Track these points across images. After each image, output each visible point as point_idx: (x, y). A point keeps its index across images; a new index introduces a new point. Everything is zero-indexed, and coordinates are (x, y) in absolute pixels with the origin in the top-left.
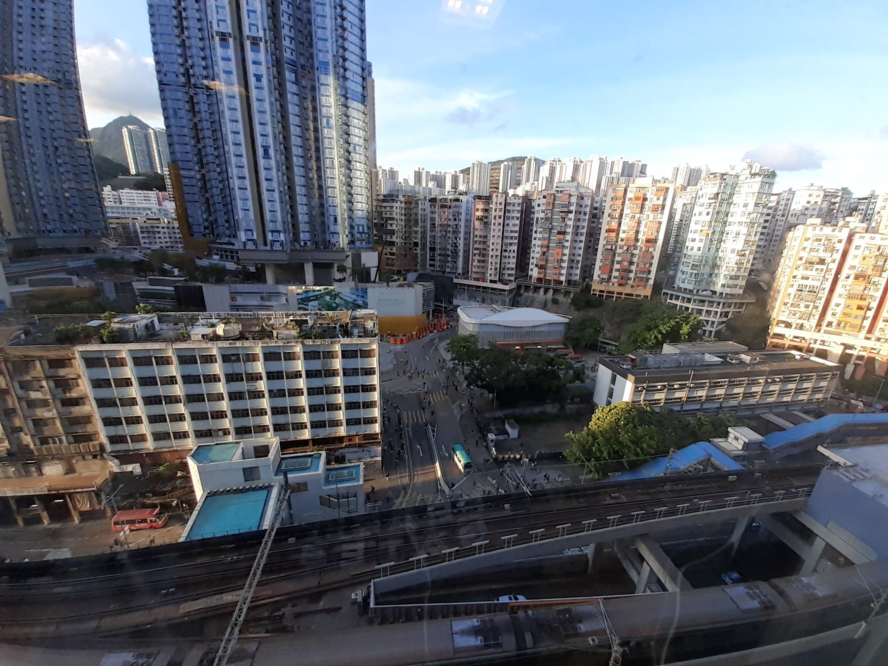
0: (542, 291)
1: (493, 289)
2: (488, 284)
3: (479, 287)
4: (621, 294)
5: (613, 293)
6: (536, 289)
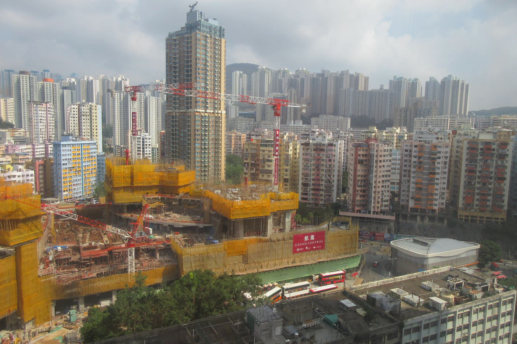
0: (418, 218)
1: (376, 219)
2: (371, 216)
3: (364, 218)
4: (483, 218)
5: (477, 217)
6: (414, 217)
